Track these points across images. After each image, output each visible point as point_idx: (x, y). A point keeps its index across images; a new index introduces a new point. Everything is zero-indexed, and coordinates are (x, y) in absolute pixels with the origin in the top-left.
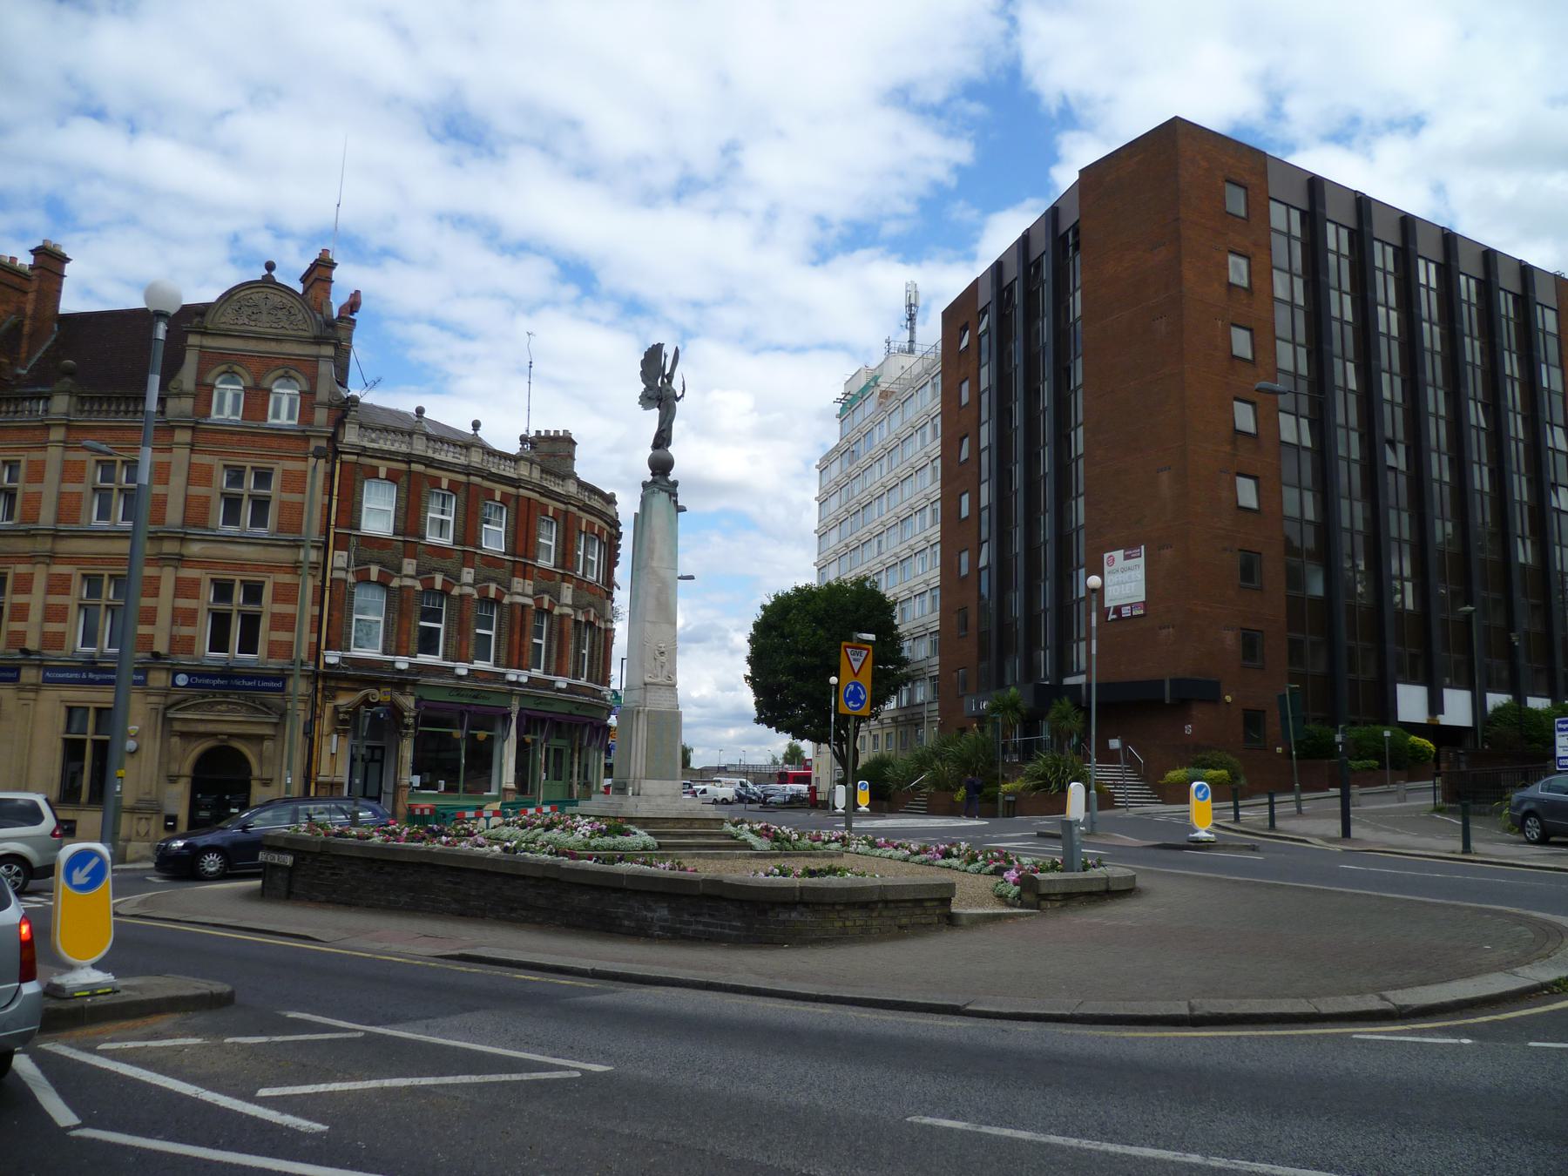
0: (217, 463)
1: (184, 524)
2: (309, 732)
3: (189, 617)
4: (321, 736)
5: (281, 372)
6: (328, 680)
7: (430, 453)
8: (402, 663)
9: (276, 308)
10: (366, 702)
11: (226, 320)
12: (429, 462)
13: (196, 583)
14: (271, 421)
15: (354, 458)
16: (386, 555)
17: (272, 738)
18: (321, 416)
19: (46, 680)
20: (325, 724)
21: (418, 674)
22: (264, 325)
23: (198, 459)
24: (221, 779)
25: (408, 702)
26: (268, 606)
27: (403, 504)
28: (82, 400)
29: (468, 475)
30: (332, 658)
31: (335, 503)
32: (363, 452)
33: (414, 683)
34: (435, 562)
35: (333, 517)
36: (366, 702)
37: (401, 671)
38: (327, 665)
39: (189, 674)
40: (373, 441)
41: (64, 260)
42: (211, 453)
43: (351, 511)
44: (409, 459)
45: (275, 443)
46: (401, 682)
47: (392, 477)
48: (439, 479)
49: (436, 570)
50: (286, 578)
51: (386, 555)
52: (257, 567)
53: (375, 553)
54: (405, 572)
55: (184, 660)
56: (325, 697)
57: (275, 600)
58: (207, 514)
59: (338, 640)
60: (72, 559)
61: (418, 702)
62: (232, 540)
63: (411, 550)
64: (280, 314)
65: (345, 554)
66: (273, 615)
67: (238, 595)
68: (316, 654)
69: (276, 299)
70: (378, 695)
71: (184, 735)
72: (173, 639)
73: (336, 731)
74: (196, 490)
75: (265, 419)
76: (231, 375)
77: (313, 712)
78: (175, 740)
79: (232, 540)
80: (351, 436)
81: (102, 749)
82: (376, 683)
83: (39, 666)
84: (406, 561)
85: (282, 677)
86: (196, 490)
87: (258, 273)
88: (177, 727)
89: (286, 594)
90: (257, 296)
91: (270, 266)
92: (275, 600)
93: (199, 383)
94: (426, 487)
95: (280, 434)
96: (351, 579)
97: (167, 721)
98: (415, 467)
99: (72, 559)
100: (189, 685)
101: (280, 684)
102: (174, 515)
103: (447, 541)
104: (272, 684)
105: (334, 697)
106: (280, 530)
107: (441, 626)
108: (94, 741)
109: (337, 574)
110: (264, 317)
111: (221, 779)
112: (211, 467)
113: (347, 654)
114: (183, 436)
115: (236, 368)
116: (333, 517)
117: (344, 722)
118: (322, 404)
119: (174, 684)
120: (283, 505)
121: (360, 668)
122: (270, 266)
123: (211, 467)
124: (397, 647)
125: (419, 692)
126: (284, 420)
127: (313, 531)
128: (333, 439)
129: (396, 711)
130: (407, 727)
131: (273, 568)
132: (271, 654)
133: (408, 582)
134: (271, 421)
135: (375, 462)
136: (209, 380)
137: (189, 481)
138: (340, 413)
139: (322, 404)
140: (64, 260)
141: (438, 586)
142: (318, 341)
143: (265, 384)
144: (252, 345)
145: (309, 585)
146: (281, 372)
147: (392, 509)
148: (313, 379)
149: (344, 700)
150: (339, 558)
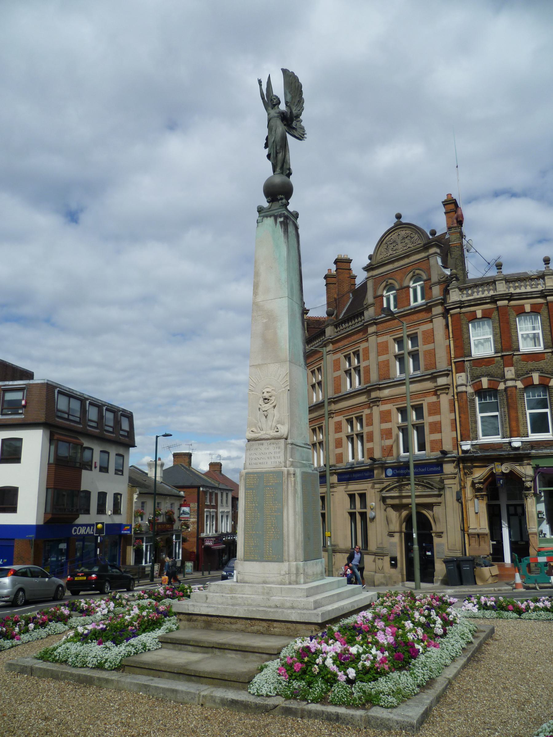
0: (389, 338)
1: (380, 379)
2: (459, 499)
3: (387, 434)
4: (466, 501)
5: (411, 274)
6: (467, 461)
7: (512, 291)
8: (517, 443)
9: (404, 238)
10: (492, 475)
11: (379, 258)
12: (510, 297)
13: (389, 412)
14: (412, 304)
15: (458, 310)
16: (492, 369)
17: (439, 504)
18: (436, 291)
19: (339, 480)
20: (469, 492)
21: (532, 448)
22: (401, 249)
23: (381, 339)
24: (420, 532)
25: (526, 470)
26: (428, 419)
27: (498, 331)
28: (336, 326)
29: (545, 297)
30: (466, 446)
31: (452, 342)
32: (461, 305)
33: (529, 457)
34: (531, 365)
35: (452, 352)
36: (492, 475)
37: (517, 449)
38: (464, 452)
39: (393, 468)
40: (468, 295)
41: (349, 261)
42: (386, 334)
43: (462, 344)
44: (494, 300)
45: (415, 317)
46: (518, 457)
47: (486, 316)
48: (523, 306)
49: (532, 371)
50: (434, 399)
51: (492, 369)
52: (415, 395)
53: (484, 369)
54: (507, 377)
55: (390, 460)
56: (465, 474)
57: (430, 414)
58: (389, 370)
59: (468, 433)
60: (340, 412)
61: (536, 468)
62: (401, 383)
63: (507, 360)
64: (407, 241)
65: (463, 374)
66: (430, 424)
67: (413, 415)
68: (457, 446)
69: (403, 233)
70: (505, 468)
71: (393, 507)
72: (383, 449)
73: (476, 497)
74: (382, 358)
75: (410, 304)
76: (390, 288)
77: (460, 485)
78: (390, 510)
79: (401, 383)
80: (455, 296)
81: (363, 515)
82: (502, 460)
83: (335, 473)
84: (506, 369)
85: (438, 465)
86: (382, 358)
87: (391, 222)
88: (389, 501)
89: (435, 409)
90: (394, 236)
91: (399, 217)
92: (430, 414)
93: (375, 297)
94: (513, 313)
95: (416, 311)
96: (470, 390)
97: (384, 499)
98: (500, 303)
99: (340, 412)
100: (393, 475)
101: (439, 469)
102: (374, 377)
103: (540, 348)
104: (435, 469)
105: (472, 473)
106: (426, 369)
107: (548, 410)
108: (359, 512)
109: (461, 389)
110: (400, 246)
111: (420, 532)
112: (387, 342)
113: (475, 442)
114: (371, 329)
115: (390, 281)
116: (452, 352)
117: (479, 490)
118: (435, 284)
119: (386, 476)
120: (426, 353)
121: (487, 450)
122: (399, 217)
123: (387, 342)
124: (511, 431)
125: (534, 463)
126: (420, 301)
127: (442, 364)
128: (443, 302)
129: (514, 479)
130: (529, 489)
131: (425, 393)
132: (432, 450)
133: (510, 383)
134: (412, 304)
135: (472, 309)
136: (379, 293)
137: (379, 354)
138: (444, 286)
139: (435, 284)
140: (349, 261)
141: (536, 381)
142: (426, 247)
143: (405, 284)
144: (397, 264)
145: (445, 400)
146: (411, 274)
147: (491, 336)
148: (428, 271)
149: (479, 473)
150: (461, 378)
